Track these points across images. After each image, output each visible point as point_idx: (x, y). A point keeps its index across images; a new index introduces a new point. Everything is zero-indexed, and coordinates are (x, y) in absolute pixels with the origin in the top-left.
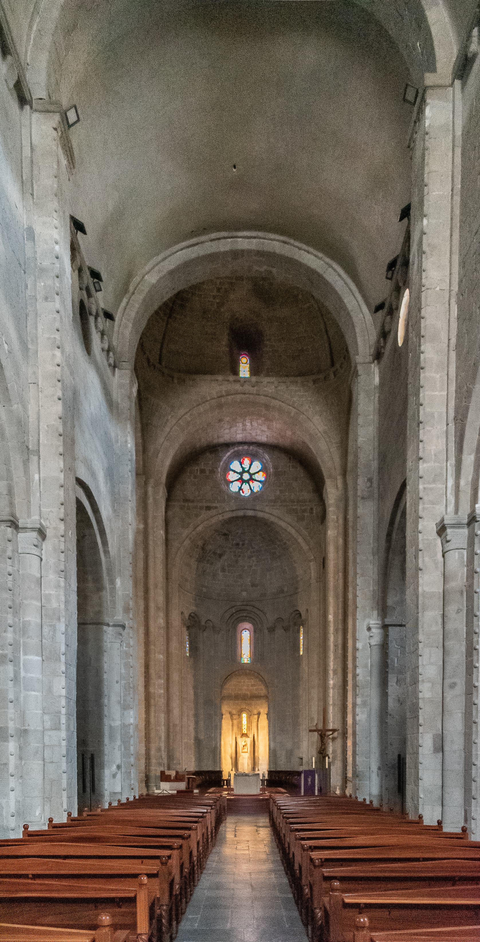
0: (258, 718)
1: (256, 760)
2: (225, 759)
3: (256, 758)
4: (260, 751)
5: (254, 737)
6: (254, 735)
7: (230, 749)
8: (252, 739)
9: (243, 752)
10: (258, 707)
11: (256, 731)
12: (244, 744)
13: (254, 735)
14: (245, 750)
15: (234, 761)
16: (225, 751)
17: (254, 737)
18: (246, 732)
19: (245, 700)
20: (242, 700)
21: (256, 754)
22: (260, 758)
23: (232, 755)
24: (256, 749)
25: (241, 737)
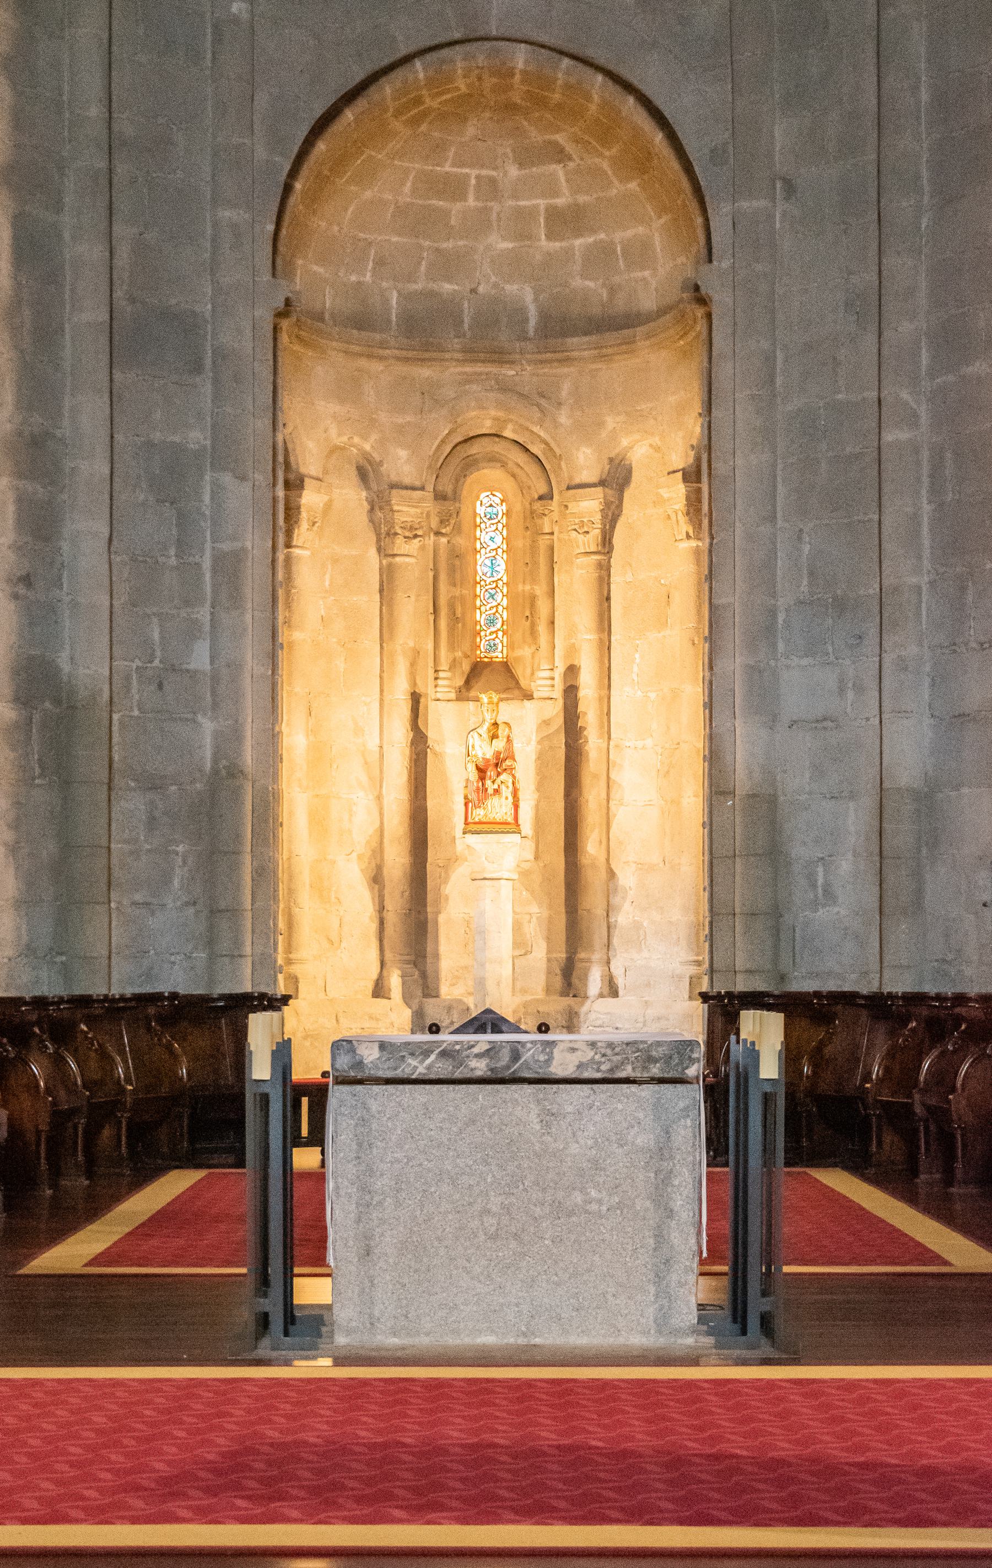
0: (611, 516)
1: (593, 901)
2: (321, 889)
3: (594, 879)
4: (622, 817)
5: (571, 692)
6: (572, 671)
7: (362, 801)
8: (555, 710)
9: (471, 827)
10: (611, 422)
11: (587, 638)
12: (484, 750)
13: (572, 671)
14: (499, 808)
15: (396, 903)
16: (319, 821)
17: (571, 692)
18: (498, 656)
19: (499, 356)
20: (471, 354)
21: (591, 847)
22: (627, 878)
23: (378, 851)
24: (592, 797)
25: (465, 691)
